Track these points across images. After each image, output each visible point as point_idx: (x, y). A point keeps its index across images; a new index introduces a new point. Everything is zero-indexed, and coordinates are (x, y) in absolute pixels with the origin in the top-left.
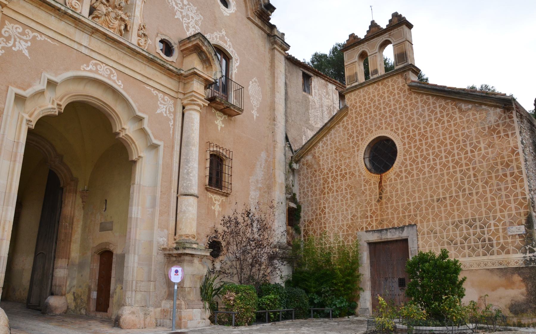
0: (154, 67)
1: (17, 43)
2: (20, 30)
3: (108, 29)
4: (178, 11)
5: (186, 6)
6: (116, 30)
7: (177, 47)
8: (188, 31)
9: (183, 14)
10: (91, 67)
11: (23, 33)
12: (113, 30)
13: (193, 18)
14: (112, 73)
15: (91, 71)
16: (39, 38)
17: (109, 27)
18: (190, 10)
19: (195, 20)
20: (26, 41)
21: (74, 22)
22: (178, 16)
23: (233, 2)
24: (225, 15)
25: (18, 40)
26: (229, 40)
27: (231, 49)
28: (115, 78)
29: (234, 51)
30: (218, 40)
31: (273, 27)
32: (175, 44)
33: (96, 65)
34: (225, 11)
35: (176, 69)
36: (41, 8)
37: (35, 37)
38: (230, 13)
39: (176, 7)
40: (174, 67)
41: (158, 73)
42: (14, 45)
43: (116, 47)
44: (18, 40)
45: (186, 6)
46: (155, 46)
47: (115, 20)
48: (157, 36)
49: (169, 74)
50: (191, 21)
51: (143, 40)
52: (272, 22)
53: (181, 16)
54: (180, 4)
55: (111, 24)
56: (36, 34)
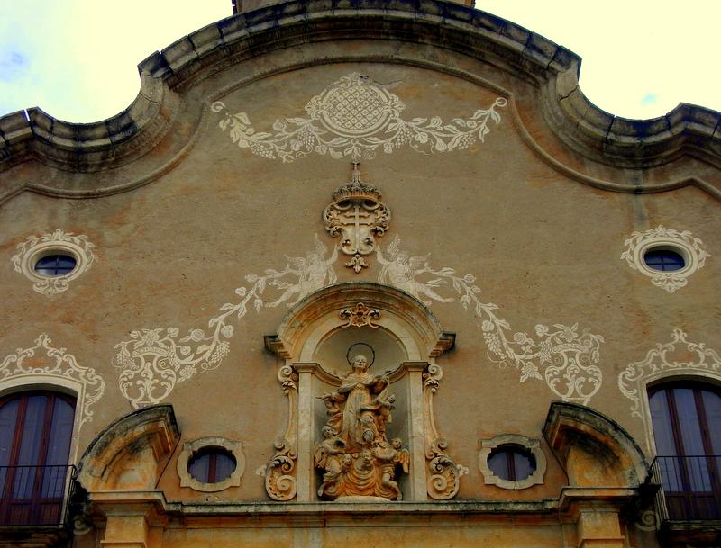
0: (484, 523)
4: (526, 361)
5: (545, 338)
7: (541, 446)
12: (370, 491)
13: (571, 355)
18: (558, 341)
19: (580, 356)
21: (283, 521)
22: (530, 372)
23: (691, 242)
24: (673, 291)
32: (532, 440)
34: (669, 280)
35: (535, 503)
36: (222, 526)
38: (688, 278)
39: (518, 358)
41: (497, 531)
43: (383, 524)
45: (545, 338)
46: (481, 473)
47: (367, 472)
48: (480, 448)
50: (569, 364)
51: (444, 480)
54: (526, 344)
55: (362, 482)
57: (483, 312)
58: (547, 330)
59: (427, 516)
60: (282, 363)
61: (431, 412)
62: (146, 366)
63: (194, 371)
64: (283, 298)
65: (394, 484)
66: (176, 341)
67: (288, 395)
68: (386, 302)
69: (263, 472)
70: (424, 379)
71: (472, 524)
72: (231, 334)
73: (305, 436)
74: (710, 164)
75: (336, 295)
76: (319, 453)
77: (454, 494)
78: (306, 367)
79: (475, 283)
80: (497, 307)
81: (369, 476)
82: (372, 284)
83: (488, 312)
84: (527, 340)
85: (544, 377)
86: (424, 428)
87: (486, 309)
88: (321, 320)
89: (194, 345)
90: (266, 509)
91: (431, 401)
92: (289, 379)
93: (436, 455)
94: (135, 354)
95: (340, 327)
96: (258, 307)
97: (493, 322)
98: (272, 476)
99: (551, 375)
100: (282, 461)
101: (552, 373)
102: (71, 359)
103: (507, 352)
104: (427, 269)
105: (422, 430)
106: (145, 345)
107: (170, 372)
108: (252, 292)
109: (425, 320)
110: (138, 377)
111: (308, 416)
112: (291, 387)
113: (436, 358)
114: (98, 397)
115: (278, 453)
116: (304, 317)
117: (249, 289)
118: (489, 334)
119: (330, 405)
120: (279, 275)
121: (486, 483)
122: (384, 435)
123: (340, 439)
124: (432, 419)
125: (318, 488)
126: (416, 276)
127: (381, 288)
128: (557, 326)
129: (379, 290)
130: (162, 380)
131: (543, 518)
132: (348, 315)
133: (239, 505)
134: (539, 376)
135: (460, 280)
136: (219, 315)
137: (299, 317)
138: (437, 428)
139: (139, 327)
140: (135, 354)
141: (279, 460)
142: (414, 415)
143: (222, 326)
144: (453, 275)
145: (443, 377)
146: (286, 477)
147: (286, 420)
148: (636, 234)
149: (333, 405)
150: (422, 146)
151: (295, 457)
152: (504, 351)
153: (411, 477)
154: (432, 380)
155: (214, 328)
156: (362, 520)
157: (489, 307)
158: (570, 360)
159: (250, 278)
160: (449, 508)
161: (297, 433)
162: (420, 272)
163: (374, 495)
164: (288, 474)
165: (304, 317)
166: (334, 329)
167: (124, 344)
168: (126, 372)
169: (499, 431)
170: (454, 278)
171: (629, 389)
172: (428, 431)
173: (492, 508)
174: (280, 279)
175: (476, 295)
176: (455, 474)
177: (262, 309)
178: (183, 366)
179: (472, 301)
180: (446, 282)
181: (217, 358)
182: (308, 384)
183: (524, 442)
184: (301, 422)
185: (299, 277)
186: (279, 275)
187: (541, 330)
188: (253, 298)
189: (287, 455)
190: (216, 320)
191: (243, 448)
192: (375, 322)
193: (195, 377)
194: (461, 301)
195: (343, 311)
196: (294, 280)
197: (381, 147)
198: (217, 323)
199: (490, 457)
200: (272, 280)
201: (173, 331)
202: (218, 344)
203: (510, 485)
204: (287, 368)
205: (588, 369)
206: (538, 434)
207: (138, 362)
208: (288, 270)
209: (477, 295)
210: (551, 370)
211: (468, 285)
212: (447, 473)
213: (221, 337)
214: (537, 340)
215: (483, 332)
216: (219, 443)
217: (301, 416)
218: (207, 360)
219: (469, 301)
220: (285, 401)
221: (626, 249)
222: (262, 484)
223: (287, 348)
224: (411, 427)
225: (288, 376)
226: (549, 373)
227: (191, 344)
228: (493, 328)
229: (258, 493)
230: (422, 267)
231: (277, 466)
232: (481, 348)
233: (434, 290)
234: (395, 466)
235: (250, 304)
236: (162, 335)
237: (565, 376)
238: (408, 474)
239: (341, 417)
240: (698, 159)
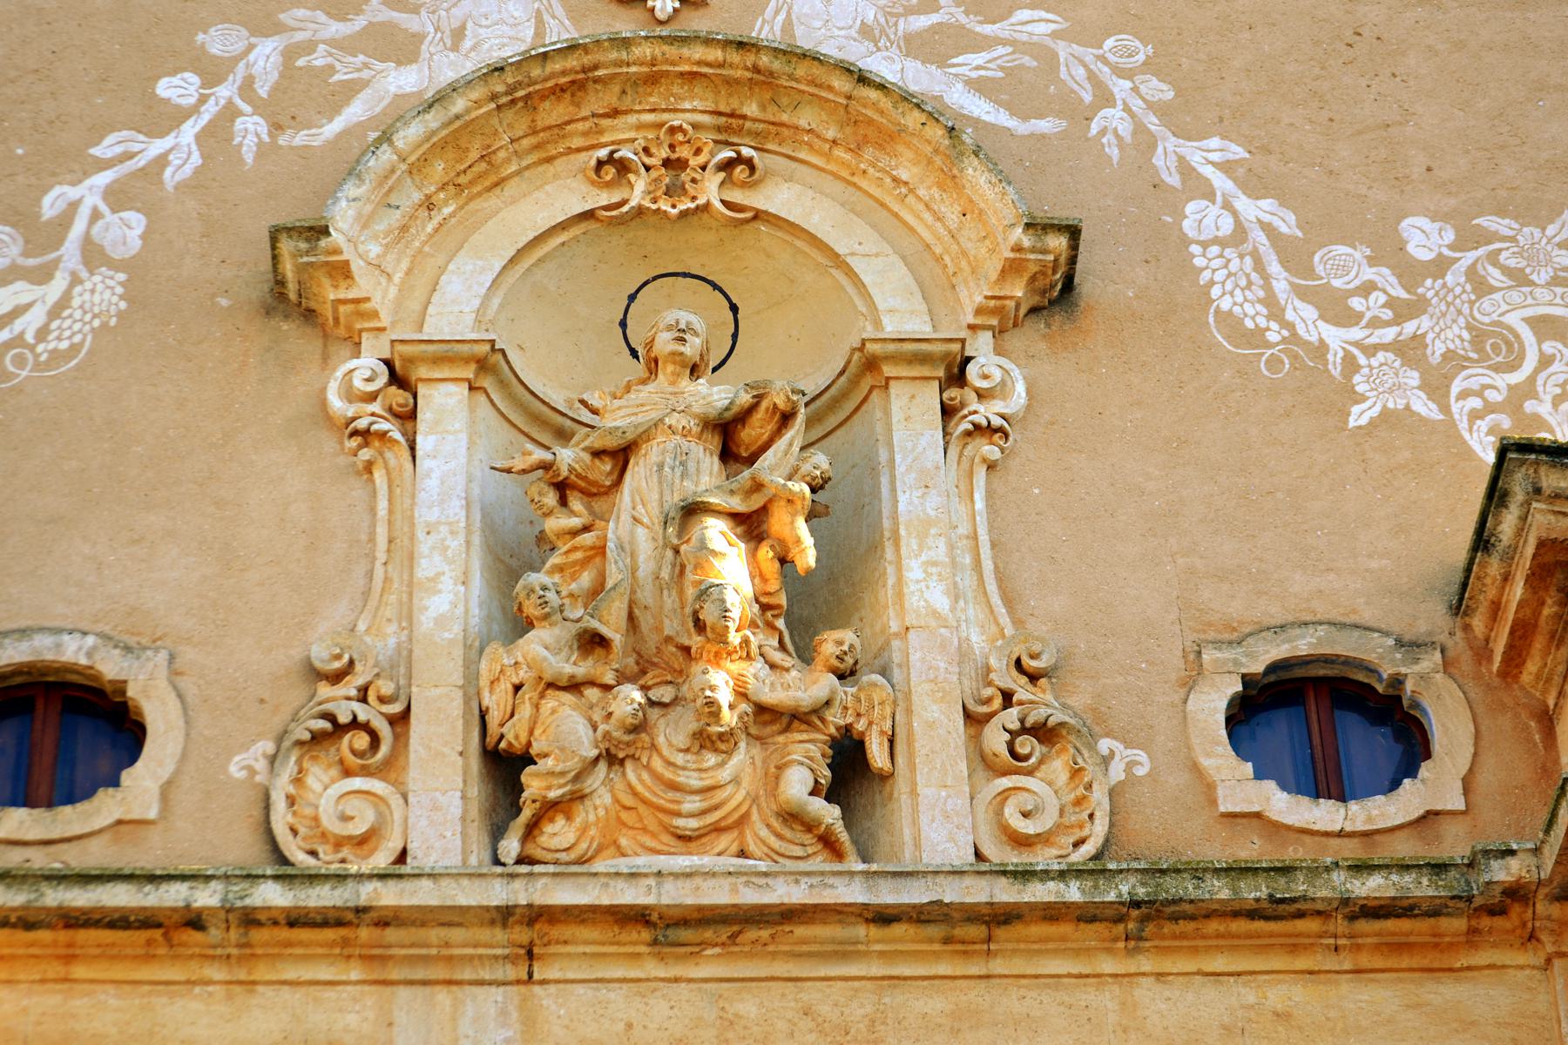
0: (1219, 963)
3: (683, 862)
4: (1370, 351)
6: (760, 832)
9: (1437, 350)
12: (724, 841)
17: (685, 839)
18: (1495, 276)
21: (346, 952)
32: (1410, 646)
36: (79, 971)
39: (1336, 337)
40: (1404, 867)
45: (1440, 266)
46: (1196, 769)
47: (711, 759)
49: (1400, 947)
50: (1545, 361)
53: (1413, 378)
54: (1367, 289)
55: (692, 804)
57: (1185, 169)
58: (1450, 236)
59: (976, 931)
60: (346, 350)
61: (984, 537)
64: (356, 111)
65: (829, 813)
67: (369, 467)
68: (785, 118)
69: (261, 765)
70: (947, 412)
71: (1168, 965)
72: (135, 243)
73: (441, 621)
75: (576, 87)
76: (505, 686)
77: (1088, 849)
78: (446, 355)
79: (1148, 66)
80: (1238, 152)
81: (725, 774)
82: (727, 43)
83: (1208, 171)
84: (1369, 273)
85: (1445, 409)
86: (956, 595)
87: (1196, 159)
88: (511, 188)
90: (272, 895)
91: (980, 504)
92: (375, 407)
93: (1008, 698)
95: (589, 215)
96: (250, 141)
97: (1227, 206)
98: (298, 781)
99: (1475, 403)
100: (344, 719)
101: (1479, 393)
103: (1290, 315)
105: (942, 544)
108: (225, 91)
109: (951, 181)
111: (456, 544)
112: (383, 435)
113: (999, 332)
115: (325, 690)
116: (439, 169)
118: (1215, 250)
119: (551, 499)
120: (336, 29)
121: (1222, 809)
122: (780, 623)
123: (595, 624)
124: (988, 565)
125: (497, 833)
126: (909, 38)
127: (764, 60)
128: (1489, 222)
129: (756, 69)
131: (1473, 937)
132: (623, 167)
133: (153, 879)
134: (1424, 407)
135: (1089, 54)
136: (87, 174)
137: (417, 168)
138: (1008, 602)
141: (330, 717)
142: (909, 543)
143: (96, 215)
144: (1055, 35)
145: (1028, 407)
146: (357, 783)
147: (360, 570)
149: (563, 502)
151: (395, 708)
152: (1275, 311)
153: (901, 785)
154: (986, 412)
156: (695, 951)
158: (1549, 347)
159: (218, 41)
160: (1073, 892)
161: (408, 616)
162: (922, 22)
163: (742, 854)
164: (366, 772)
165: (439, 169)
166: (562, 226)
169: (1276, 613)
170: (1063, 50)
172: (973, 612)
173: (1254, 891)
175: (1150, 106)
176: (1091, 770)
177: (262, 151)
179: (1139, 128)
180: (1027, 60)
181: (73, 331)
182: (459, 423)
183: (1384, 660)
184: (426, 567)
185: (419, 38)
186: (336, 29)
188: (230, 113)
189: (363, 699)
190: (73, 193)
191: (174, 673)
192: (736, 196)
194: (1095, 128)
195: (603, 153)
196: (404, 50)
198: (74, 206)
199: (1231, 722)
200: (309, 47)
202: (75, 280)
203: (1325, 814)
204: (365, 367)
206: (1432, 618)
210: (1474, 384)
211: (1120, 72)
212: (1058, 768)
213: (93, 254)
214: (1410, 272)
215: (1186, 241)
216: (73, 651)
217: (425, 545)
218: (30, 338)
219: (1125, 129)
220: (358, 491)
222: (257, 813)
223: (364, 284)
224: (900, 595)
225: (372, 397)
226: (1464, 395)
228: (1227, 225)
229: (242, 849)
231: (317, 738)
233: (979, 86)
234: (835, 743)
235: (217, 135)
237: (1530, 406)
238: (885, 778)
239: (600, 550)
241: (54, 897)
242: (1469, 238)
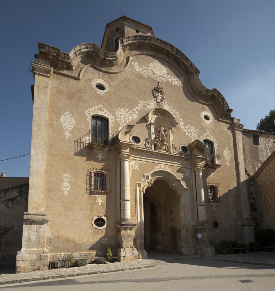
1: (135, 167)
2: (135, 162)
8: (192, 138)
10: (158, 167)
11: (136, 163)
13: (193, 132)
14: (166, 166)
15: (159, 168)
16: (141, 162)
20: (137, 165)
25: (135, 165)
26: (211, 135)
27: (213, 138)
28: (167, 168)
29: (214, 139)
30: (206, 137)
31: (233, 119)
33: (160, 165)
37: (139, 163)
42: (134, 168)
44: (135, 165)
52: (232, 116)
56: (140, 161)
62: (122, 117)
63: (131, 120)
64: (147, 108)
66: (127, 112)
74: (214, 102)
89: (131, 114)
94: (119, 113)
95: (157, 117)
102: (107, 111)
104: (171, 109)
106: (121, 112)
107: (127, 119)
108: (141, 105)
110: (121, 118)
114: (113, 121)
117: (140, 104)
120: (146, 103)
130: (125, 120)
139: (120, 107)
140: (119, 113)
148: (203, 112)
150: (170, 82)
154: (173, 131)
155: (134, 111)
157: (181, 120)
159: (140, 102)
167: (117, 110)
168: (118, 117)
171: (201, 140)
174: (146, 104)
177: (143, 109)
178: (129, 118)
181: (135, 118)
186: (146, 103)
187: (189, 126)
188: (141, 107)
193: (132, 121)
196: (149, 105)
197: (163, 80)
201: (127, 110)
205: (196, 135)
207: (120, 115)
208: (147, 102)
209: (180, 117)
213: (136, 114)
216: (137, 136)
221: (202, 114)
227: (130, 113)
230: (170, 108)
232: (180, 127)
235: (141, 108)
236: (125, 110)
240: (212, 100)
241: (140, 149)
242: (191, 127)
